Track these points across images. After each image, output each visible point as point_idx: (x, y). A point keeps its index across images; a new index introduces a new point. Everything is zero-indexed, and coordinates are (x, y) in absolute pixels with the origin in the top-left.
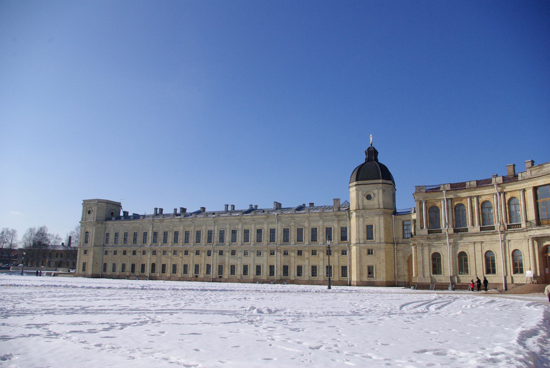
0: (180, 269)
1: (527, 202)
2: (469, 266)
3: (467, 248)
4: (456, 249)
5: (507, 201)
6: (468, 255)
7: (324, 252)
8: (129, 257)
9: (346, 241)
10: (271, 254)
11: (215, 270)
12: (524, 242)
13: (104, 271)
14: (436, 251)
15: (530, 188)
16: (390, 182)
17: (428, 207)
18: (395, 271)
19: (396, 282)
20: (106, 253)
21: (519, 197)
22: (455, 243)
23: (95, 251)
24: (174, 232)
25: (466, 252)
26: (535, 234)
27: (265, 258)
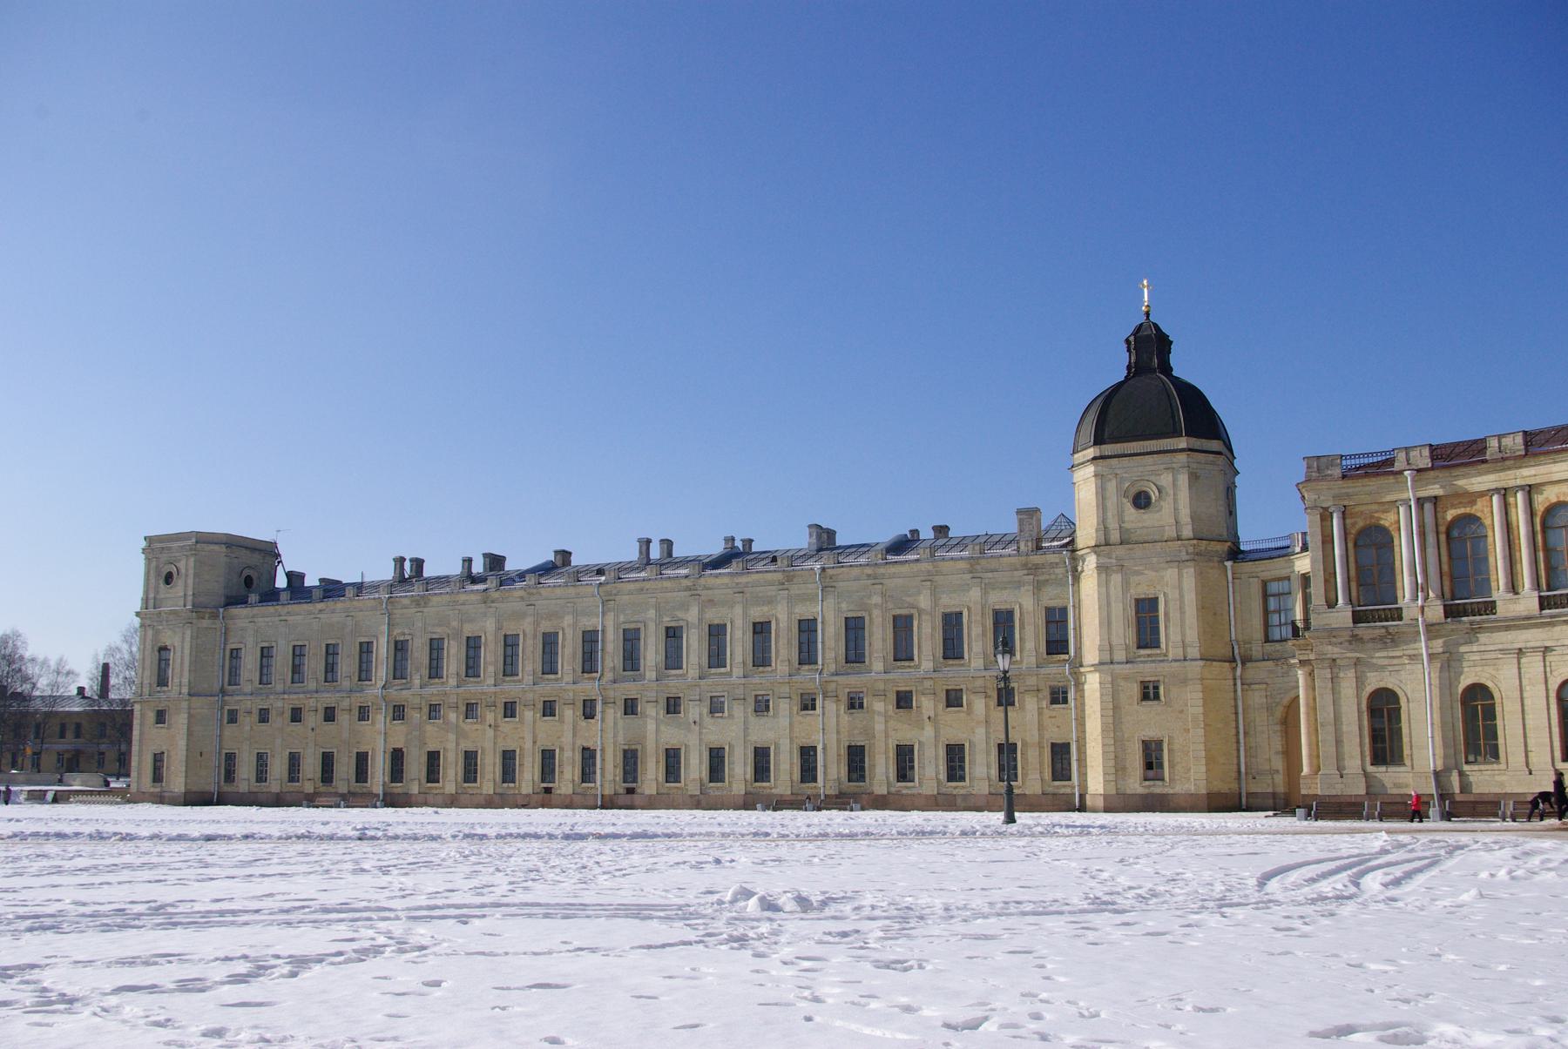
0: (490, 767)
2: (1500, 733)
3: (1493, 672)
7: (990, 697)
8: (313, 729)
9: (1066, 657)
10: (805, 708)
11: (610, 766)
13: (225, 782)
14: (1382, 685)
16: (1215, 445)
17: (1353, 532)
18: (1238, 757)
19: (1244, 794)
20: (233, 718)
22: (1451, 653)
23: (192, 711)
24: (465, 638)
25: (1489, 684)
27: (784, 722)
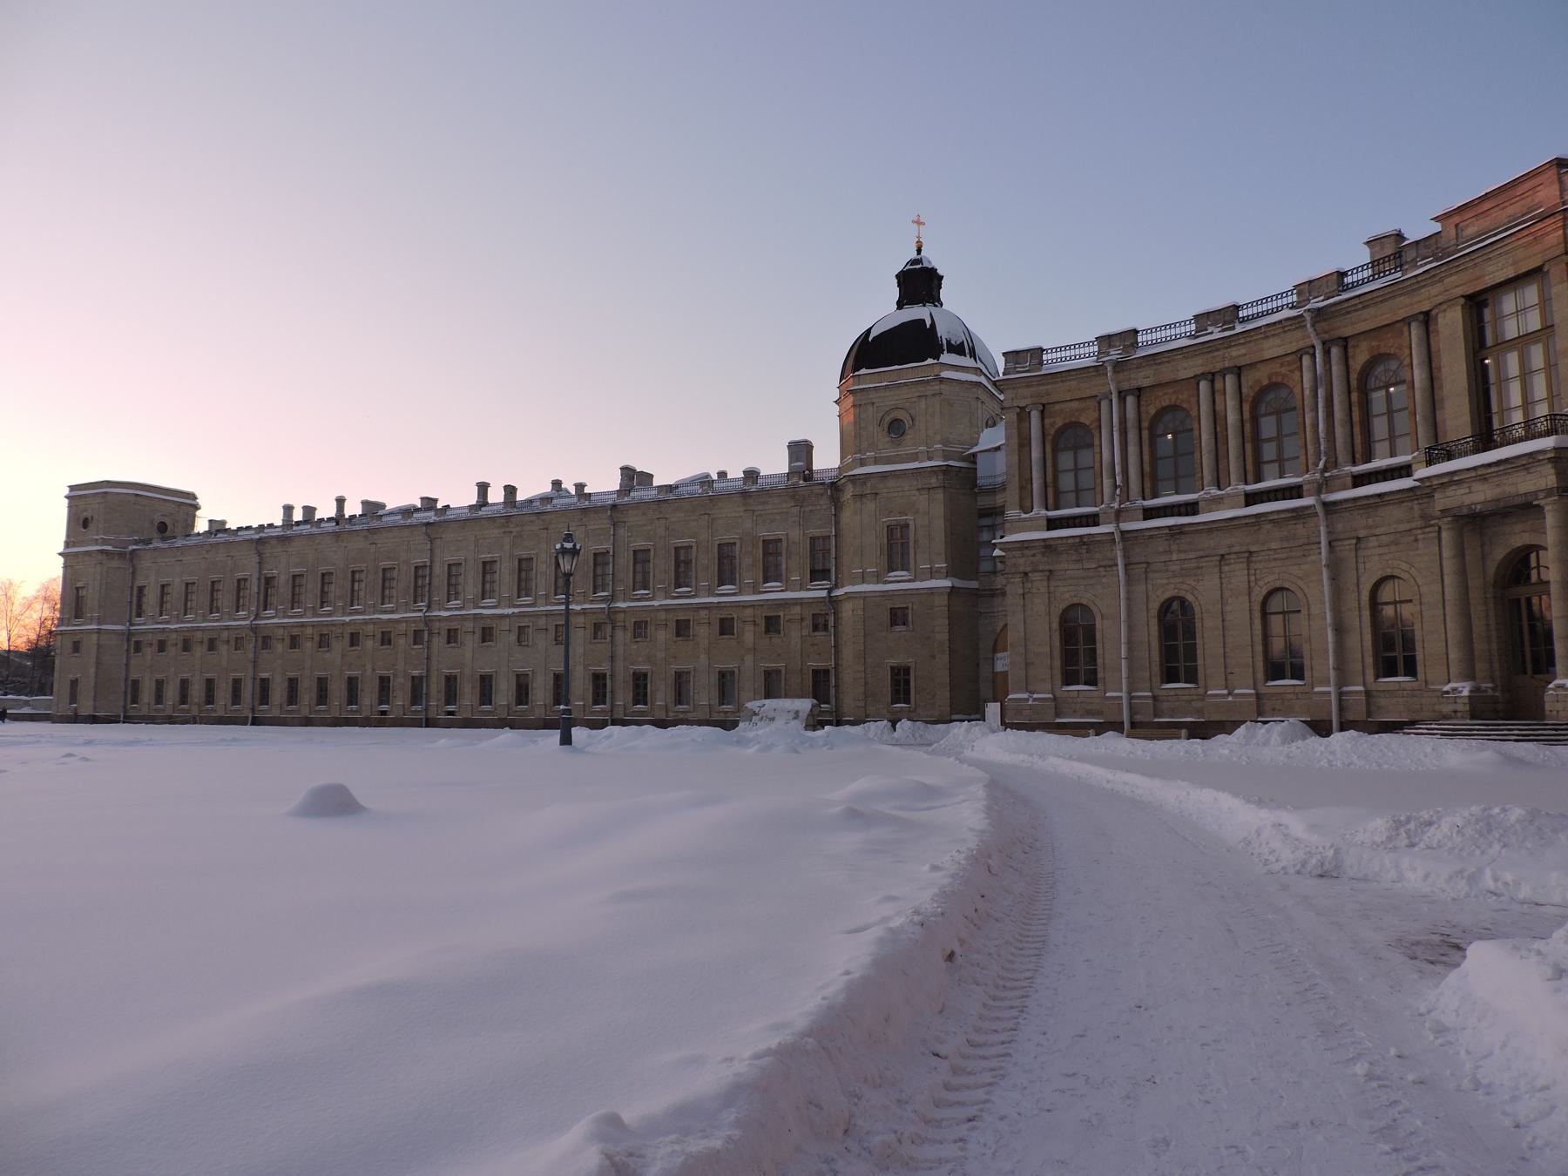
0: (338, 690)
1: (1439, 369)
2: (1199, 652)
3: (1193, 583)
4: (1150, 587)
5: (1354, 377)
6: (1197, 609)
7: (758, 625)
12: (1421, 545)
15: (1450, 302)
17: (1052, 432)
21: (1407, 351)
22: (1148, 563)
24: (320, 575)
25: (1189, 597)
26: (1468, 500)
